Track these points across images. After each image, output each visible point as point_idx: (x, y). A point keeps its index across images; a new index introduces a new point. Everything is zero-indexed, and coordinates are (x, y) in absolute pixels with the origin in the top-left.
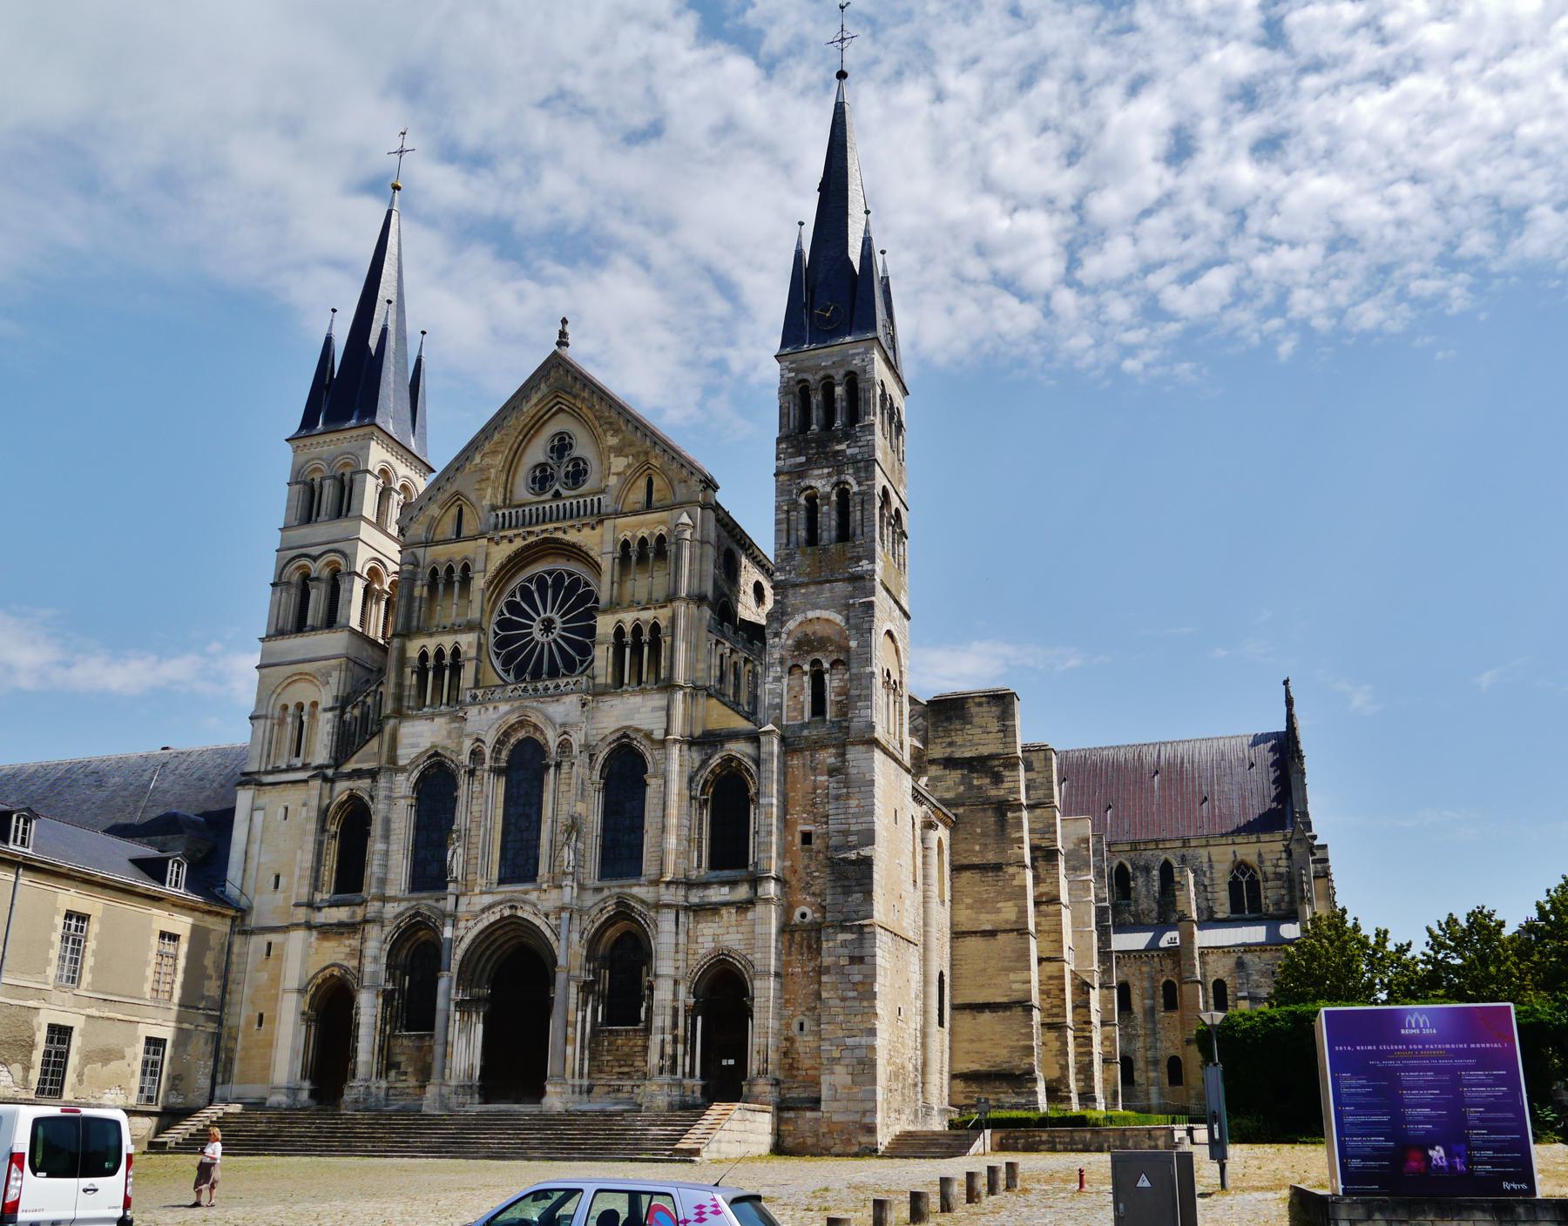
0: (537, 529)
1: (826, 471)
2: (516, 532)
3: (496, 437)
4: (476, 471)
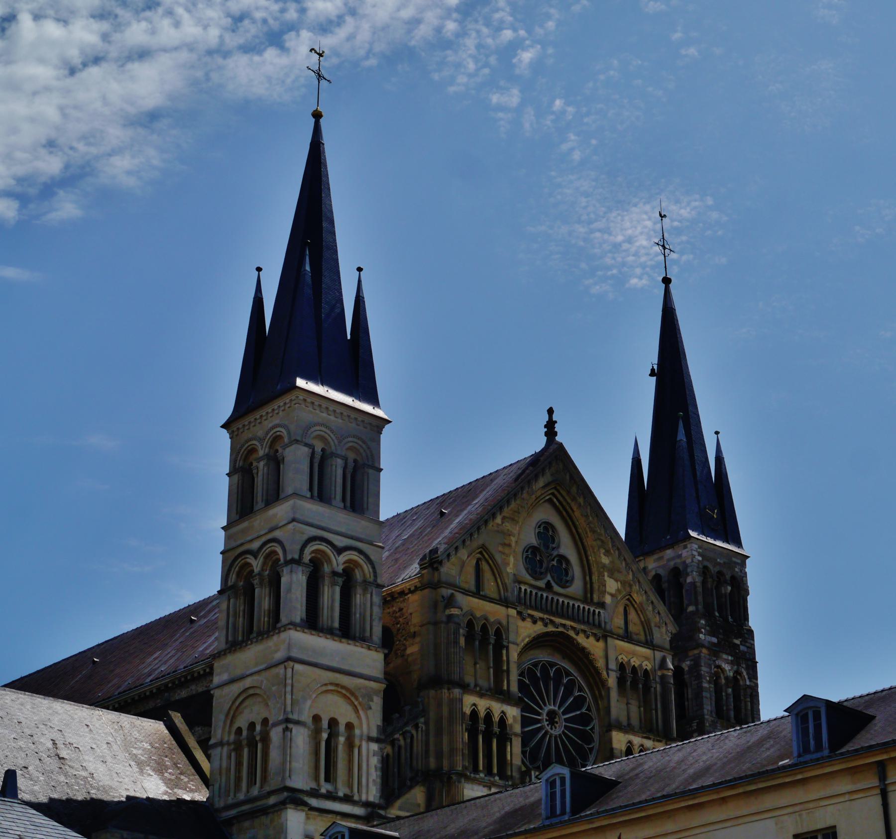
0: (558, 620)
1: (730, 658)
2: (541, 615)
3: (513, 505)
4: (498, 531)
